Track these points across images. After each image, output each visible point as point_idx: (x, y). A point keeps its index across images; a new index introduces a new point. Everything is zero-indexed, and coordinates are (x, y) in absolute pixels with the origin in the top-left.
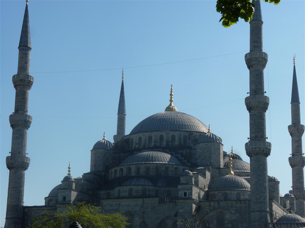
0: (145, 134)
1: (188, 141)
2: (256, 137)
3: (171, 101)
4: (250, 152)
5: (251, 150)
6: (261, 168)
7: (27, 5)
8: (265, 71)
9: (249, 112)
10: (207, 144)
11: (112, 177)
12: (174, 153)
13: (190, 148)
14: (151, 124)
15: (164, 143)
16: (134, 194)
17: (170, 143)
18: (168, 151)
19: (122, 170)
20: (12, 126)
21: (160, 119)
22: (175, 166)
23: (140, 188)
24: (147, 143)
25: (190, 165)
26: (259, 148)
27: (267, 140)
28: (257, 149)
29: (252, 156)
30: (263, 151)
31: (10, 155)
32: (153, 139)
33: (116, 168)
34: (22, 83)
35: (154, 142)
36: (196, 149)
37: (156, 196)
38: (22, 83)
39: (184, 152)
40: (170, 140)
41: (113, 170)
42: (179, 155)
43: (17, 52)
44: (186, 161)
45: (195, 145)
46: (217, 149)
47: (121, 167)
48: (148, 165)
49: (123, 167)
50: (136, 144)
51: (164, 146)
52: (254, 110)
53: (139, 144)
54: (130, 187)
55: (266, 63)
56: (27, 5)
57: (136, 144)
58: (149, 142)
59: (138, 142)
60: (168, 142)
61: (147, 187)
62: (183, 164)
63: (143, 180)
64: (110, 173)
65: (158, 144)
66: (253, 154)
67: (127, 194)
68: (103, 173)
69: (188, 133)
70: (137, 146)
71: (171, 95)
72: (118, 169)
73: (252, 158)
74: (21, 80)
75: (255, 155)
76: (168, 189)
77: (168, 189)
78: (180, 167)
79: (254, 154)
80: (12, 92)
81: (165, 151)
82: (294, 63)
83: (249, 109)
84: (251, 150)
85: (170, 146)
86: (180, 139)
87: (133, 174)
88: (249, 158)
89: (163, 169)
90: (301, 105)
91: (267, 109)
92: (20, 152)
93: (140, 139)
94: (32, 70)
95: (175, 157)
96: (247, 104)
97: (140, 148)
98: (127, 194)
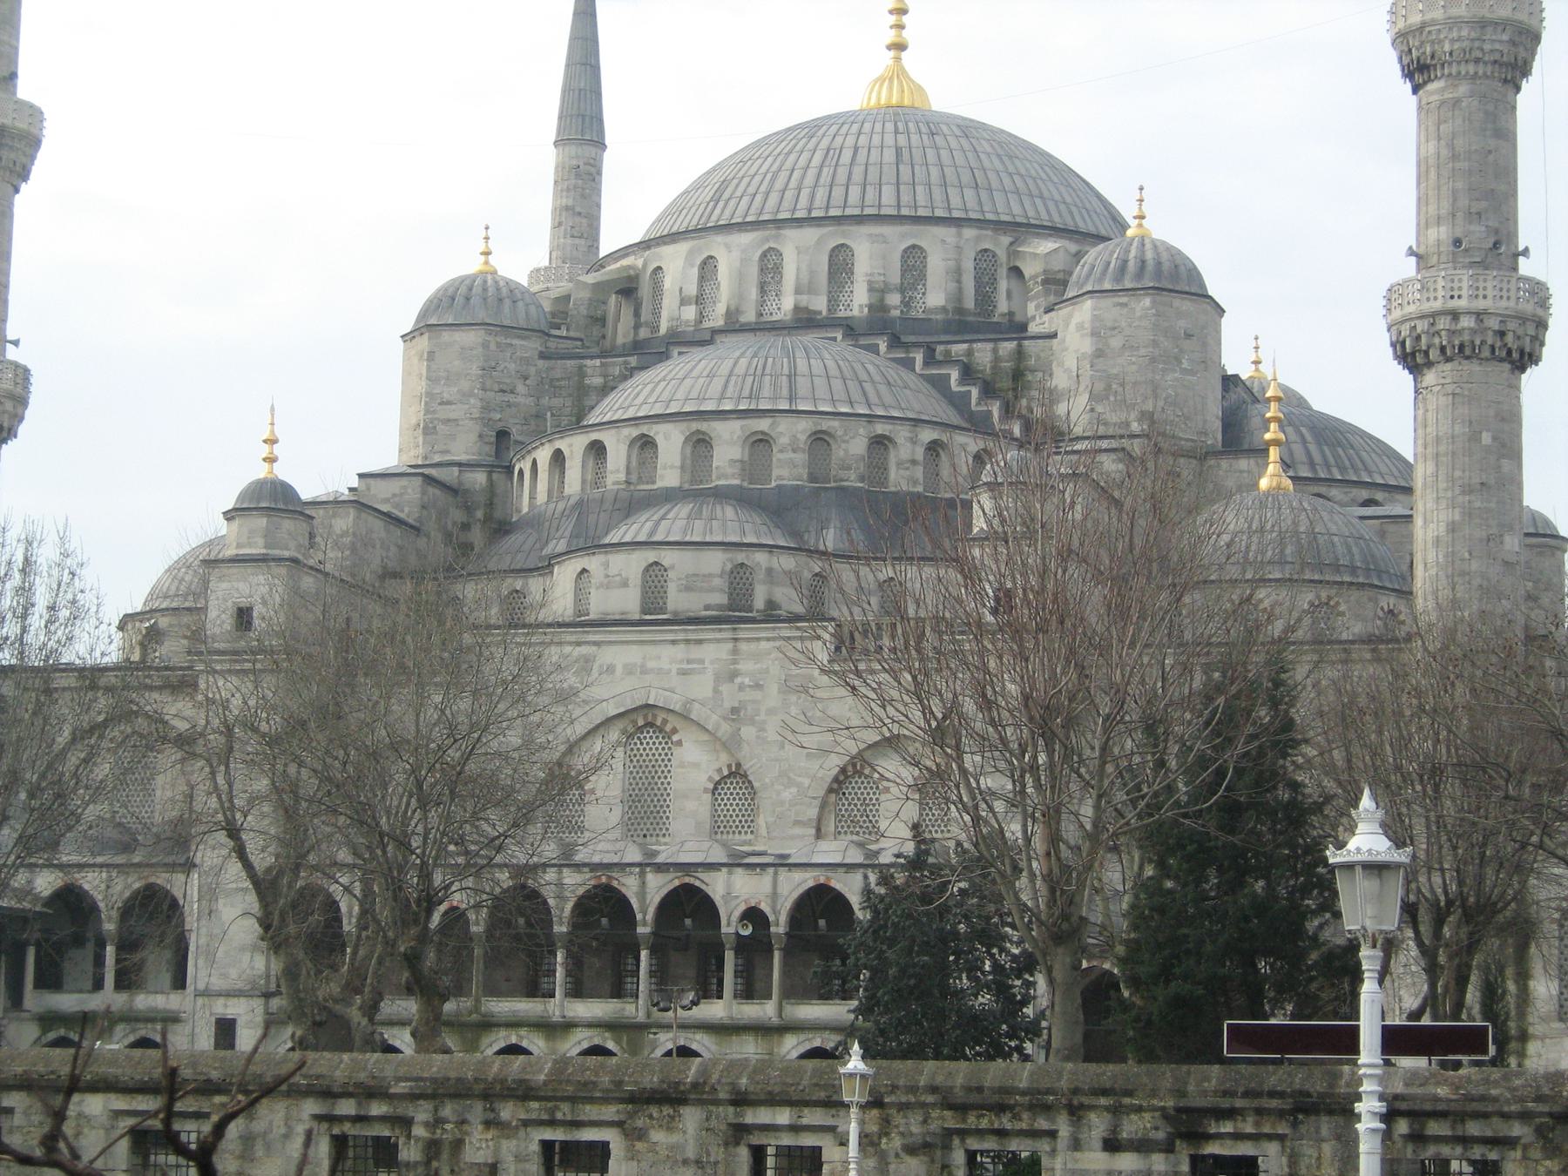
1: (1003, 285)
2: (1457, 242)
4: (1418, 338)
5: (1422, 326)
6: (1486, 438)
9: (1415, 90)
10: (1124, 305)
11: (532, 497)
12: (919, 358)
13: (1017, 328)
15: (858, 301)
16: (677, 600)
17: (894, 299)
18: (883, 347)
19: (597, 449)
22: (928, 435)
23: (715, 562)
24: (753, 293)
25: (1017, 431)
26: (1479, 315)
27: (1525, 267)
28: (1466, 322)
29: (1429, 364)
30: (1502, 334)
33: (562, 444)
35: (798, 291)
36: (1054, 336)
37: (816, 614)
39: (983, 354)
40: (895, 278)
42: (955, 375)
44: (995, 409)
45: (1048, 310)
46: (1188, 336)
47: (594, 436)
48: (763, 424)
49: (608, 438)
50: (684, 302)
51: (856, 312)
52: (1450, 75)
53: (699, 300)
54: (651, 556)
57: (684, 302)
58: (763, 289)
59: (692, 289)
60: (878, 291)
61: (761, 558)
62: (978, 424)
63: (730, 512)
64: (521, 472)
65: (820, 304)
66: (1434, 354)
67: (628, 601)
68: (479, 478)
70: (690, 313)
72: (574, 446)
73: (1430, 378)
75: (1449, 360)
76: (887, 572)
77: (887, 572)
78: (960, 438)
79: (1443, 349)
81: (863, 341)
83: (1417, 71)
84: (1422, 326)
85: (896, 313)
86: (957, 273)
88: (1406, 378)
89: (857, 446)
93: (707, 268)
96: (1402, 39)
97: (707, 324)
98: (628, 601)
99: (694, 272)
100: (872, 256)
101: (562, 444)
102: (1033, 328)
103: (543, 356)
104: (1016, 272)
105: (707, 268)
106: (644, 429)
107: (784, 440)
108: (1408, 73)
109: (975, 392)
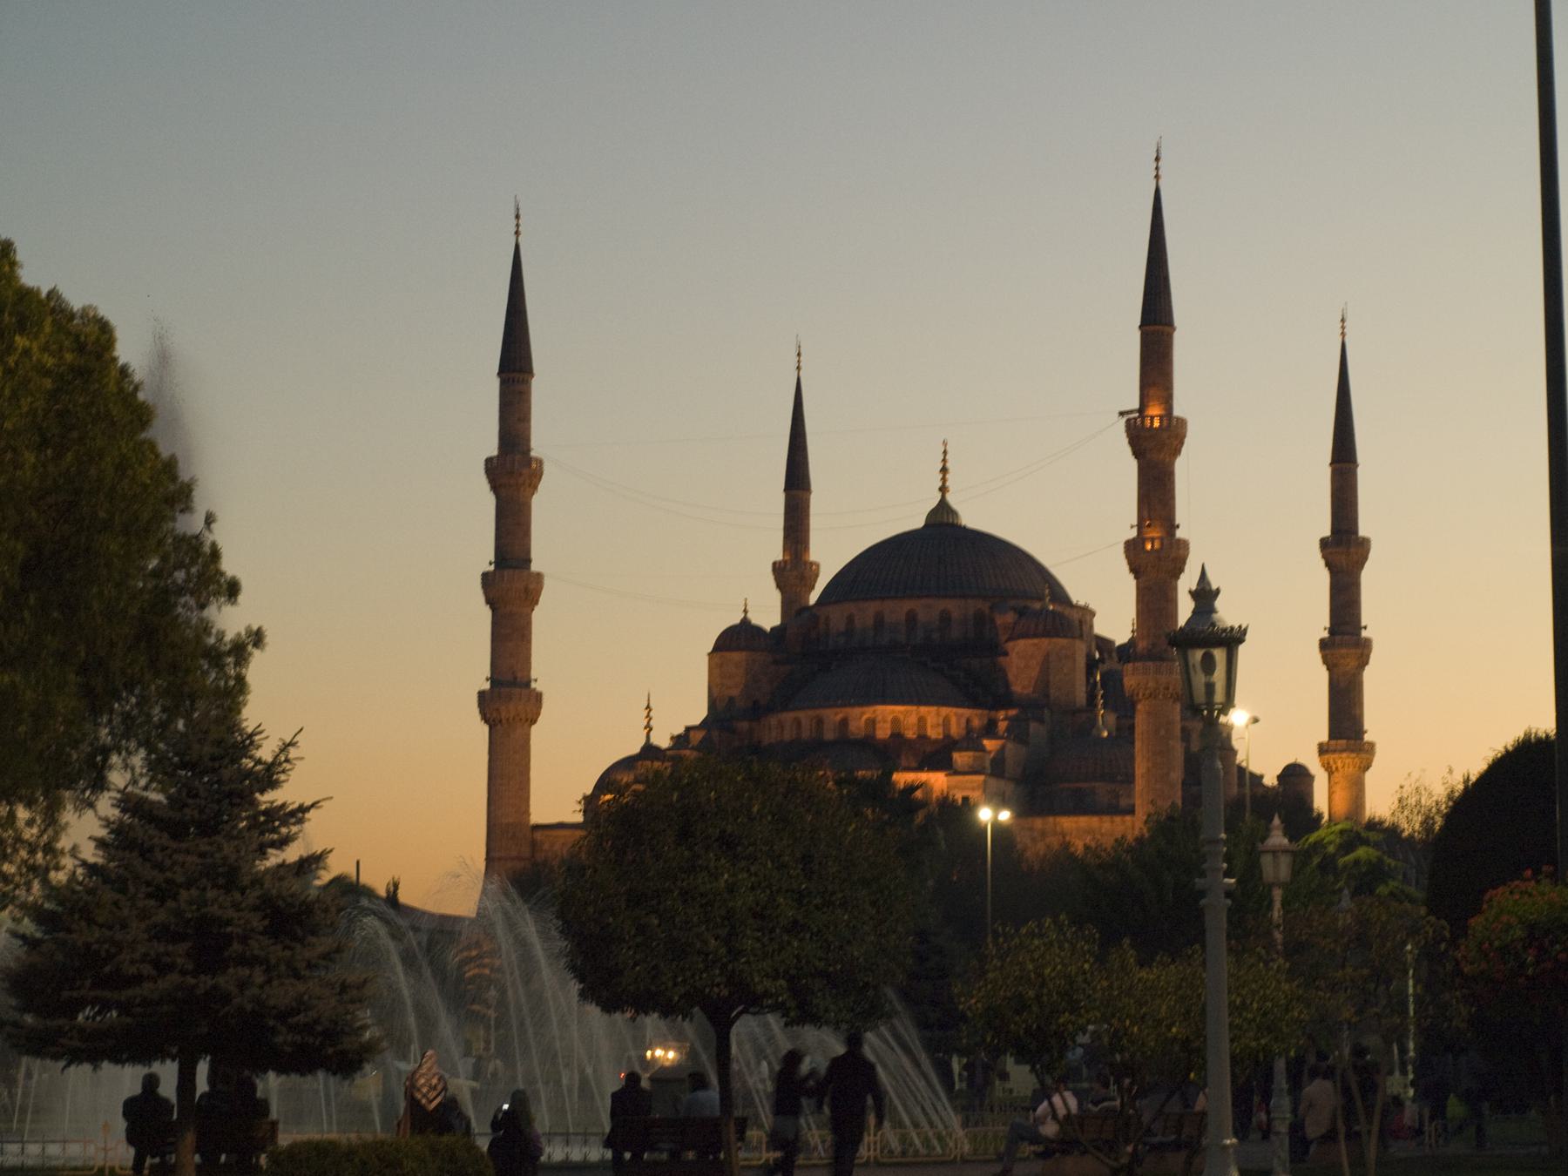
3: (943, 489)
8: (1180, 465)
14: (881, 566)
17: (935, 636)
31: (487, 686)
41: (773, 720)
43: (493, 385)
55: (1182, 443)
71: (944, 470)
72: (788, 717)
80: (485, 503)
82: (1343, 334)
83: (1135, 570)
90: (1362, 473)
91: (1181, 570)
93: (850, 619)
94: (541, 442)
105: (850, 619)
108: (1132, 570)
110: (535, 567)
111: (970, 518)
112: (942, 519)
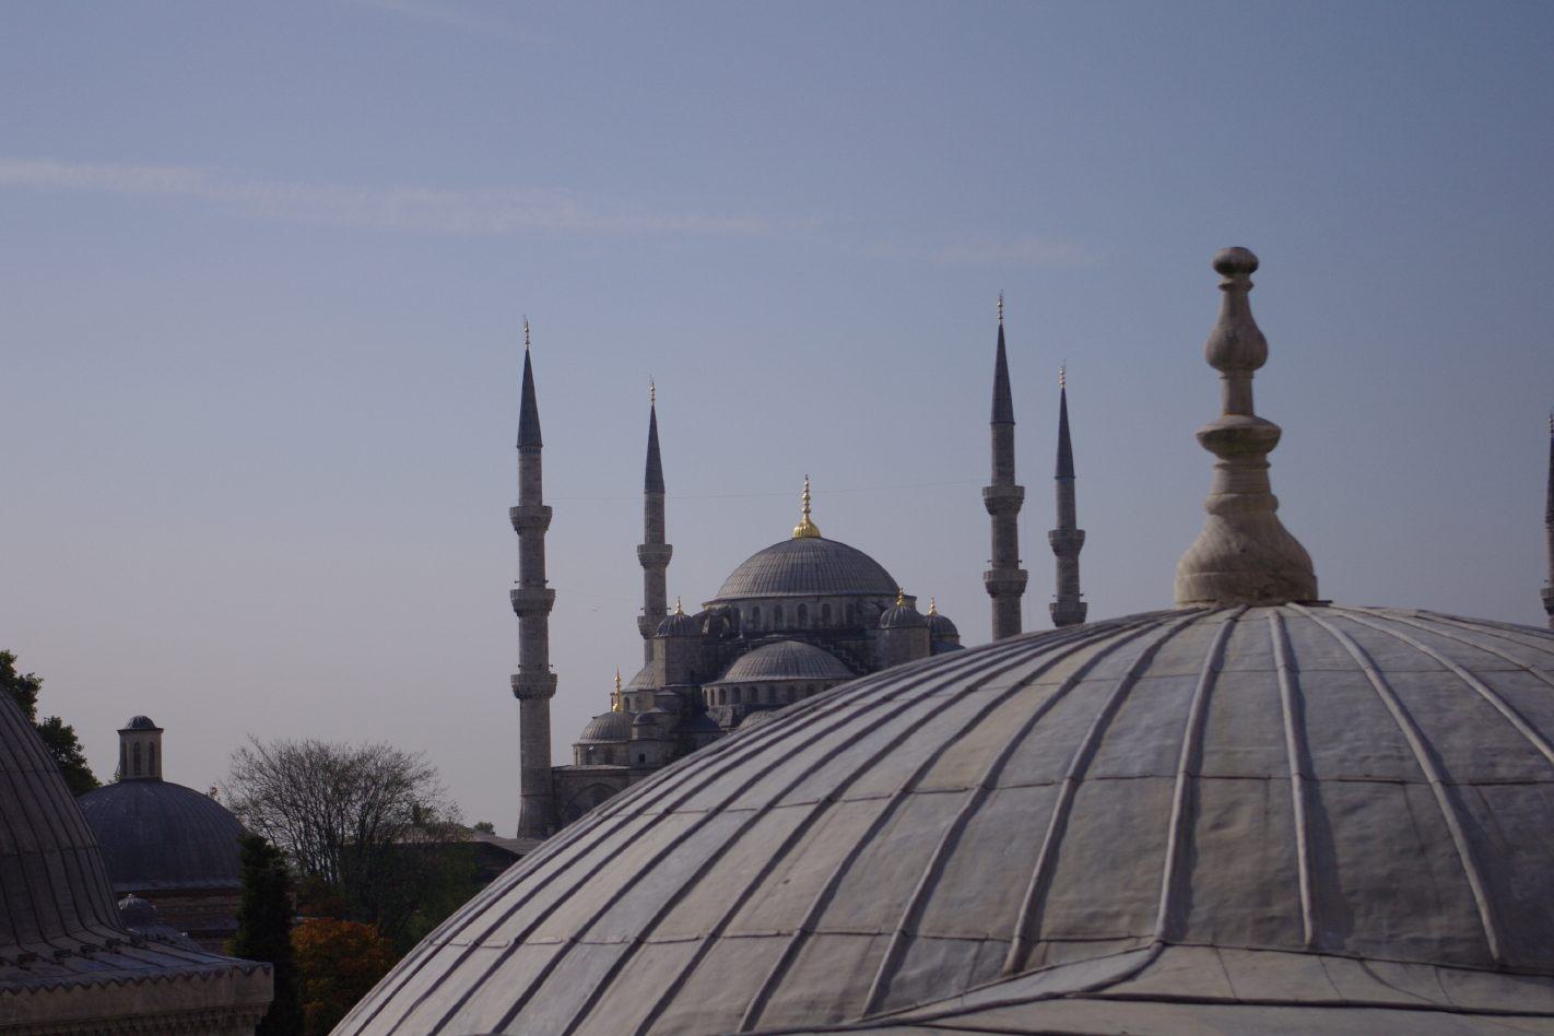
0: (766, 601)
7: (527, 352)
12: (832, 647)
13: (862, 631)
15: (810, 622)
20: (519, 612)
21: (793, 564)
31: (517, 671)
32: (785, 614)
34: (531, 521)
38: (531, 521)
39: (852, 644)
40: (820, 615)
42: (844, 652)
44: (858, 664)
48: (789, 684)
50: (748, 622)
53: (753, 621)
56: (527, 352)
57: (748, 622)
58: (776, 619)
65: (796, 625)
69: (856, 600)
74: (533, 518)
87: (763, 701)
91: (1023, 591)
92: (540, 665)
95: (836, 656)
99: (751, 612)
100: (814, 610)
101: (725, 688)
102: (868, 633)
103: (703, 644)
104: (860, 612)
106: (754, 685)
107: (799, 688)
109: (851, 659)
110: (548, 586)
111: (830, 532)
112: (811, 533)
